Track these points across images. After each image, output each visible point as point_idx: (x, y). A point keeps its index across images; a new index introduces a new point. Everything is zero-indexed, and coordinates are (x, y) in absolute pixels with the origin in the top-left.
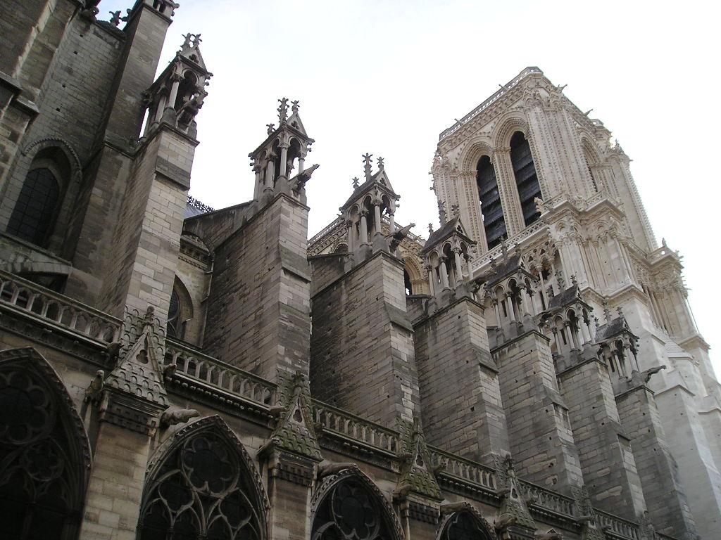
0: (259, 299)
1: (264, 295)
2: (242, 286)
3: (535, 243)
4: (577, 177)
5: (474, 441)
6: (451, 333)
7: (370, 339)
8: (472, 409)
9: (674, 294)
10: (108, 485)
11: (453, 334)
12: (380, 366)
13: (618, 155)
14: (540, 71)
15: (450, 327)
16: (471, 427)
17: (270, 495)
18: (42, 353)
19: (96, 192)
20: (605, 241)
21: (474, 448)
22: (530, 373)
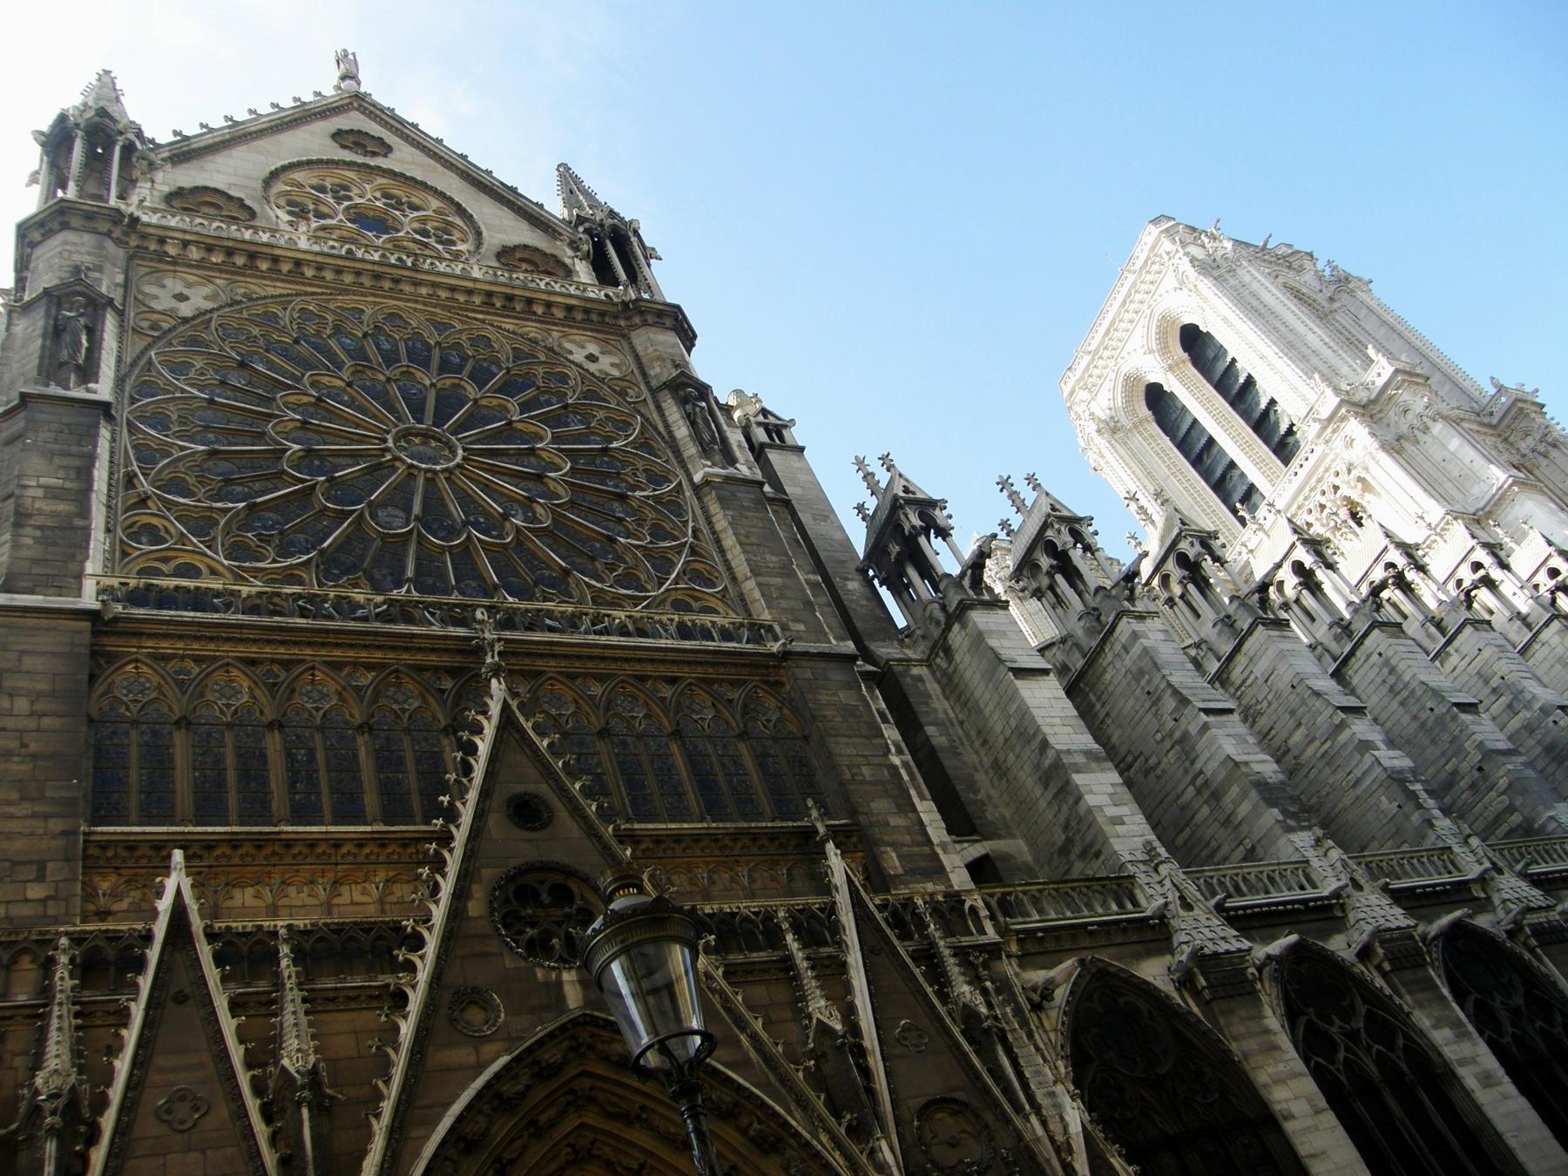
0: (1187, 763)
1: (1192, 756)
2: (1135, 760)
3: (1319, 480)
4: (1327, 353)
5: (1511, 809)
6: (1379, 680)
7: (1317, 743)
8: (1480, 769)
9: (1554, 453)
10: (1270, 1070)
11: (1384, 681)
12: (1358, 773)
13: (1343, 283)
14: (1170, 219)
15: (1372, 675)
16: (1493, 793)
17: (1401, 997)
18: (1104, 956)
19: (931, 730)
20: (1426, 430)
21: (1516, 819)
22: (1495, 682)
